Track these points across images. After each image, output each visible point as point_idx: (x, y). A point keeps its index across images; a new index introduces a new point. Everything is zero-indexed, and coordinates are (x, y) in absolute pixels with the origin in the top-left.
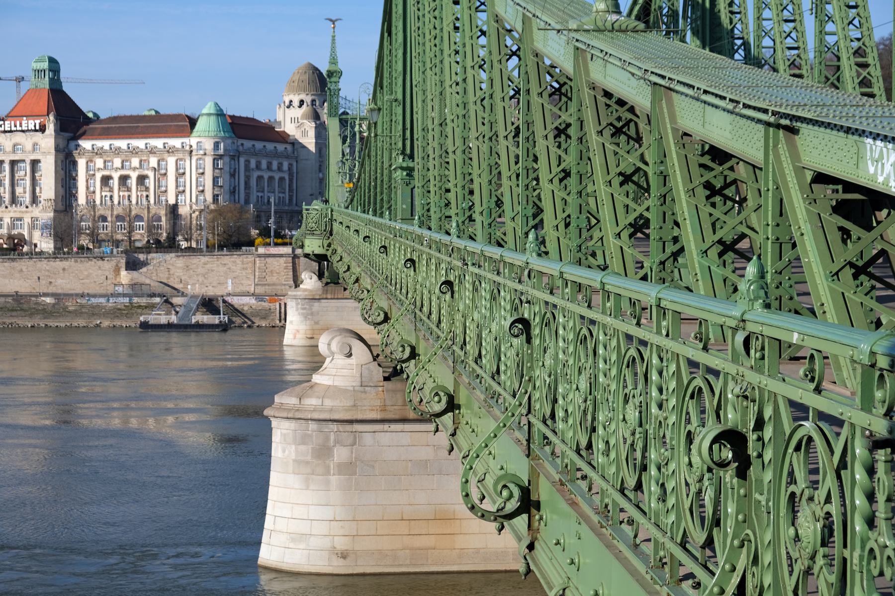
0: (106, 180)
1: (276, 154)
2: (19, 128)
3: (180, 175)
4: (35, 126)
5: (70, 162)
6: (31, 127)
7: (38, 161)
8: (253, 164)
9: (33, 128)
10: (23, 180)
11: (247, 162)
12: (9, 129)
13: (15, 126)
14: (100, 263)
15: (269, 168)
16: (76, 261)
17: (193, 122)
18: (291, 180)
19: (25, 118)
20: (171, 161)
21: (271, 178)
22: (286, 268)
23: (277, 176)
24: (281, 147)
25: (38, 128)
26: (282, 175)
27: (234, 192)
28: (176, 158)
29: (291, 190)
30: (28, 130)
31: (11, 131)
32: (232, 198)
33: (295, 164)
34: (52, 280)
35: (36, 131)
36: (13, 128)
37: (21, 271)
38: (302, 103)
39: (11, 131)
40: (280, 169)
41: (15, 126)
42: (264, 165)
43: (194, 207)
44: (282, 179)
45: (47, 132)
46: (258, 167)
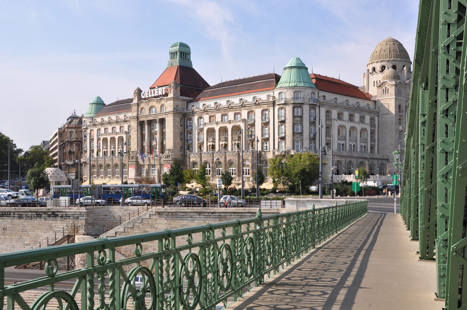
0: (211, 132)
1: (358, 109)
2: (153, 95)
5: (187, 119)
6: (160, 93)
8: (334, 114)
9: (161, 94)
17: (277, 78)
18: (372, 133)
20: (258, 112)
23: (359, 127)
24: (363, 103)
26: (363, 126)
27: (314, 139)
30: (158, 96)
31: (149, 98)
32: (313, 145)
33: (376, 118)
38: (383, 68)
43: (277, 153)
44: (363, 130)
45: (169, 96)
46: (340, 116)
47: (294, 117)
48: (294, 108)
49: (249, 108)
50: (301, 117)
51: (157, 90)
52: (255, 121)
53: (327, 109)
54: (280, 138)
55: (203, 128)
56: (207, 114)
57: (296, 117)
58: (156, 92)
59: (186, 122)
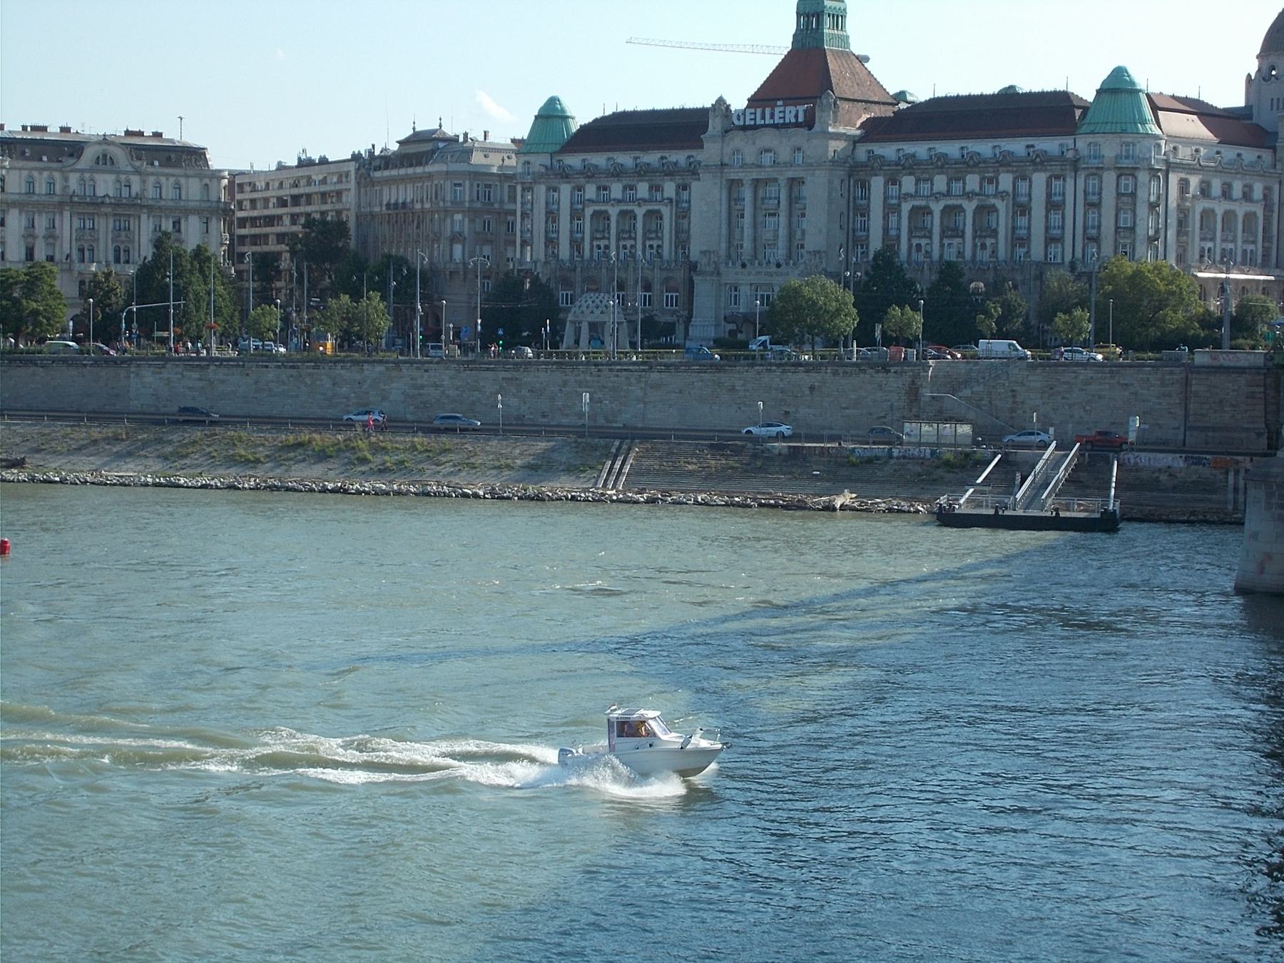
3: (1053, 205)
4: (796, 116)
5: (856, 182)
6: (790, 118)
7: (801, 181)
9: (793, 120)
10: (774, 215)
11: (1184, 186)
12: (752, 123)
13: (763, 117)
14: (880, 377)
15: (1226, 194)
16: (835, 373)
19: (779, 103)
21: (1229, 216)
22: (1251, 396)
23: (1241, 209)
25: (801, 119)
28: (1048, 174)
29: (1267, 238)
30: (785, 126)
31: (755, 127)
33: (1276, 187)
34: (791, 410)
35: (797, 125)
36: (759, 122)
37: (733, 389)
39: (755, 127)
40: (1247, 196)
41: (763, 117)
42: (1216, 188)
44: (1250, 217)
47: (1119, 195)
48: (1119, 177)
49: (1016, 171)
50: (1133, 195)
51: (782, 109)
52: (1031, 200)
53: (1183, 175)
54: (1088, 239)
55: (899, 205)
56: (910, 174)
57: (1124, 195)
58: (777, 115)
59: (852, 189)
